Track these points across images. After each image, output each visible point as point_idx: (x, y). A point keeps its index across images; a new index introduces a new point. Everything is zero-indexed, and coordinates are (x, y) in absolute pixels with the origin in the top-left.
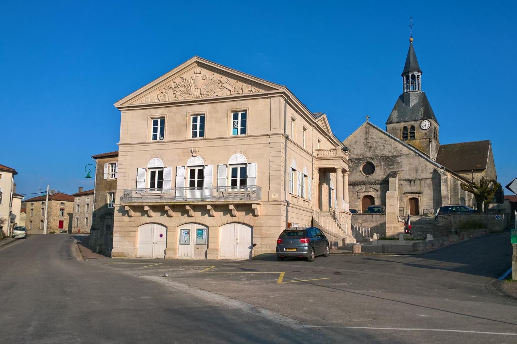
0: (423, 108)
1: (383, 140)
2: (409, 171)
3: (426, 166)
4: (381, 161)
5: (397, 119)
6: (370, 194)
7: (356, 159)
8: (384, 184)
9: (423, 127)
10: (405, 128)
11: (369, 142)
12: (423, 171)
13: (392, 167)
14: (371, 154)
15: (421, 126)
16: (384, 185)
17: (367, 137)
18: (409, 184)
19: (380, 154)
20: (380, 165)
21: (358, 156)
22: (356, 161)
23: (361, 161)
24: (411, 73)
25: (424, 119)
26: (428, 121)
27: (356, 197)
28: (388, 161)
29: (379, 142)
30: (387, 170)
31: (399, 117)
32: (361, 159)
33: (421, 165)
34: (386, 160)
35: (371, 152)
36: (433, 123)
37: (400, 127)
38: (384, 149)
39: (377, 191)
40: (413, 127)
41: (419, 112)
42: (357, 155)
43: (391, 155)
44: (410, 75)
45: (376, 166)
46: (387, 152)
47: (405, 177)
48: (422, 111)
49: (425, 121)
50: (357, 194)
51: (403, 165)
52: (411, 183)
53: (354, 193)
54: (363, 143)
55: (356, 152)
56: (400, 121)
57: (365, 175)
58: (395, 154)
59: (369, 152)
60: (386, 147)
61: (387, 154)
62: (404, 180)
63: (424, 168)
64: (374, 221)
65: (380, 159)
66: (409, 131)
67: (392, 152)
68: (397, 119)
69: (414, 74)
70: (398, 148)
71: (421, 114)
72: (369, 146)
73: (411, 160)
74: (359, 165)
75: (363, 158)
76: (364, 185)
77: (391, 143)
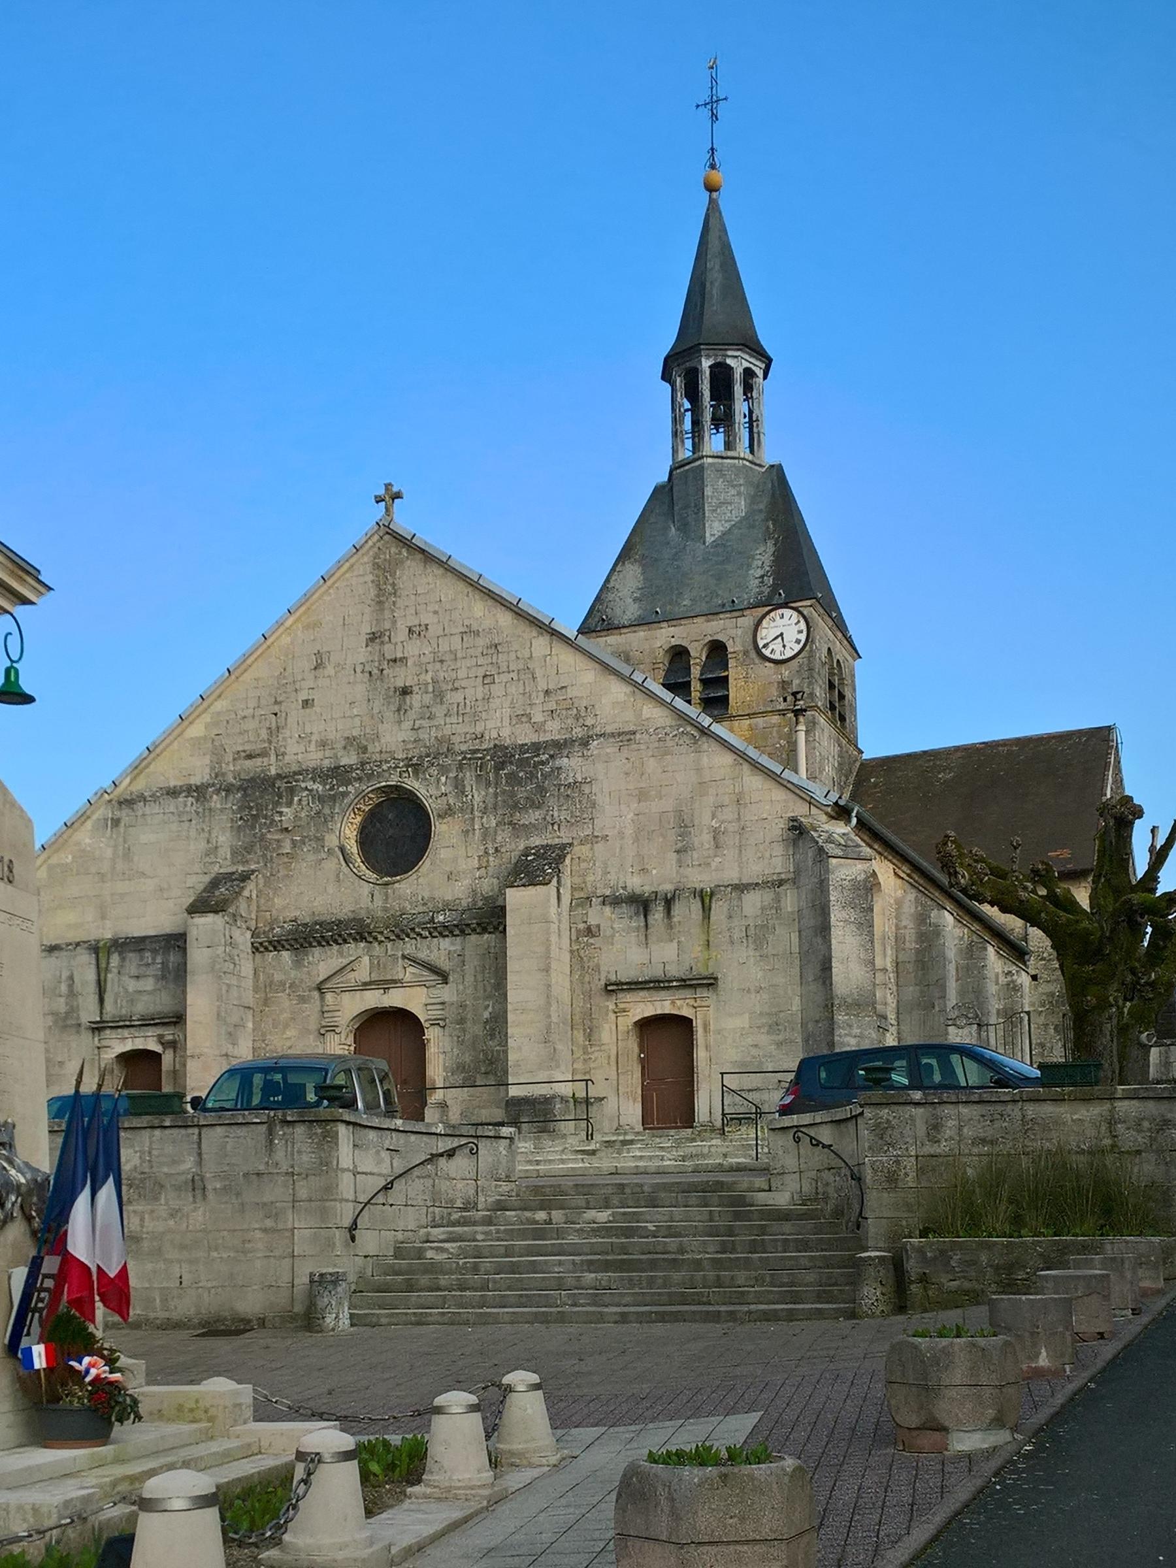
0: (770, 543)
1: (481, 642)
2: (636, 840)
3: (739, 801)
4: (469, 777)
5: (636, 605)
6: (395, 999)
7: (319, 774)
8: (484, 930)
9: (771, 647)
10: (679, 654)
11: (399, 655)
12: (722, 838)
13: (533, 816)
14: (411, 736)
15: (761, 644)
16: (486, 936)
17: (387, 625)
18: (638, 929)
19: (459, 732)
20: (462, 810)
21: (328, 753)
22: (318, 787)
23: (348, 783)
24: (708, 357)
25: (776, 600)
26: (795, 614)
27: (313, 1025)
28: (513, 778)
29: (459, 655)
30: (503, 835)
31: (647, 594)
32: (349, 769)
33: (710, 800)
34: (497, 774)
35: (407, 725)
36: (823, 627)
37: (652, 651)
38: (487, 699)
39: (444, 977)
40: (717, 650)
41: (749, 566)
42: (323, 744)
43: (526, 736)
44: (706, 364)
45: (439, 816)
46: (506, 722)
47: (613, 877)
48: (767, 563)
49: (780, 611)
50: (322, 999)
51: (599, 799)
52: (645, 916)
53: (303, 999)
54: (359, 670)
55: (316, 729)
56: (653, 618)
57: (371, 876)
58: (554, 731)
59: (400, 722)
60: (497, 690)
61: (506, 732)
62: (604, 903)
63: (729, 814)
64: (213, 1185)
65: (460, 767)
66: (696, 672)
67: (538, 717)
68: (636, 605)
69: (729, 361)
70: (571, 693)
71: (762, 577)
72: (400, 683)
73: (652, 764)
74: (332, 808)
75: (363, 764)
76: (363, 939)
77: (531, 657)
